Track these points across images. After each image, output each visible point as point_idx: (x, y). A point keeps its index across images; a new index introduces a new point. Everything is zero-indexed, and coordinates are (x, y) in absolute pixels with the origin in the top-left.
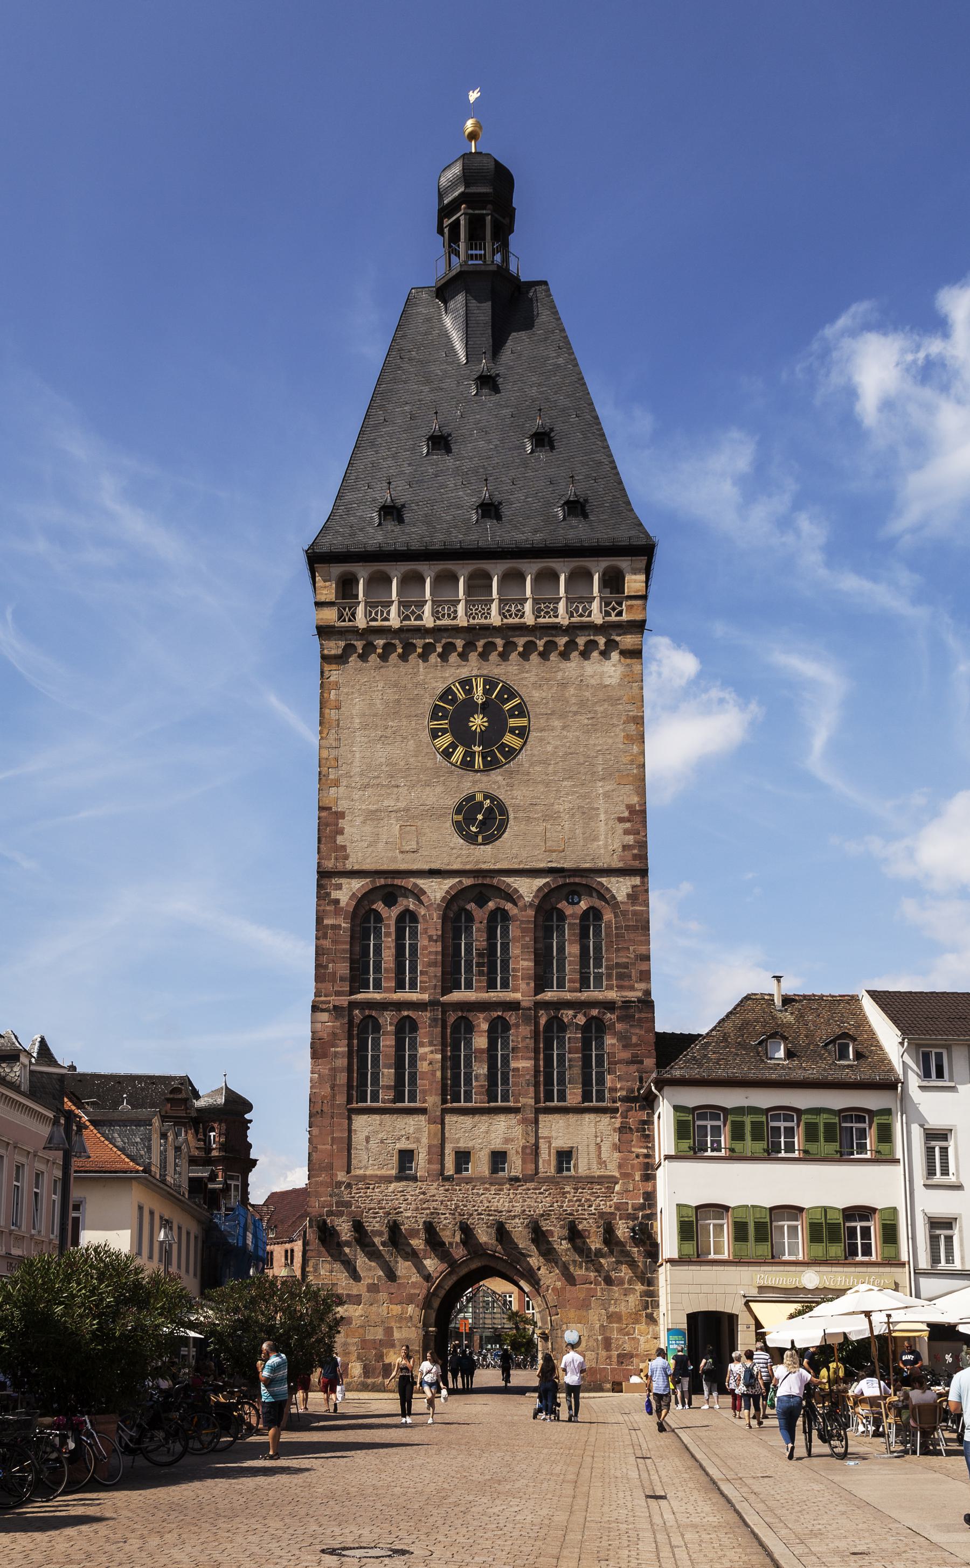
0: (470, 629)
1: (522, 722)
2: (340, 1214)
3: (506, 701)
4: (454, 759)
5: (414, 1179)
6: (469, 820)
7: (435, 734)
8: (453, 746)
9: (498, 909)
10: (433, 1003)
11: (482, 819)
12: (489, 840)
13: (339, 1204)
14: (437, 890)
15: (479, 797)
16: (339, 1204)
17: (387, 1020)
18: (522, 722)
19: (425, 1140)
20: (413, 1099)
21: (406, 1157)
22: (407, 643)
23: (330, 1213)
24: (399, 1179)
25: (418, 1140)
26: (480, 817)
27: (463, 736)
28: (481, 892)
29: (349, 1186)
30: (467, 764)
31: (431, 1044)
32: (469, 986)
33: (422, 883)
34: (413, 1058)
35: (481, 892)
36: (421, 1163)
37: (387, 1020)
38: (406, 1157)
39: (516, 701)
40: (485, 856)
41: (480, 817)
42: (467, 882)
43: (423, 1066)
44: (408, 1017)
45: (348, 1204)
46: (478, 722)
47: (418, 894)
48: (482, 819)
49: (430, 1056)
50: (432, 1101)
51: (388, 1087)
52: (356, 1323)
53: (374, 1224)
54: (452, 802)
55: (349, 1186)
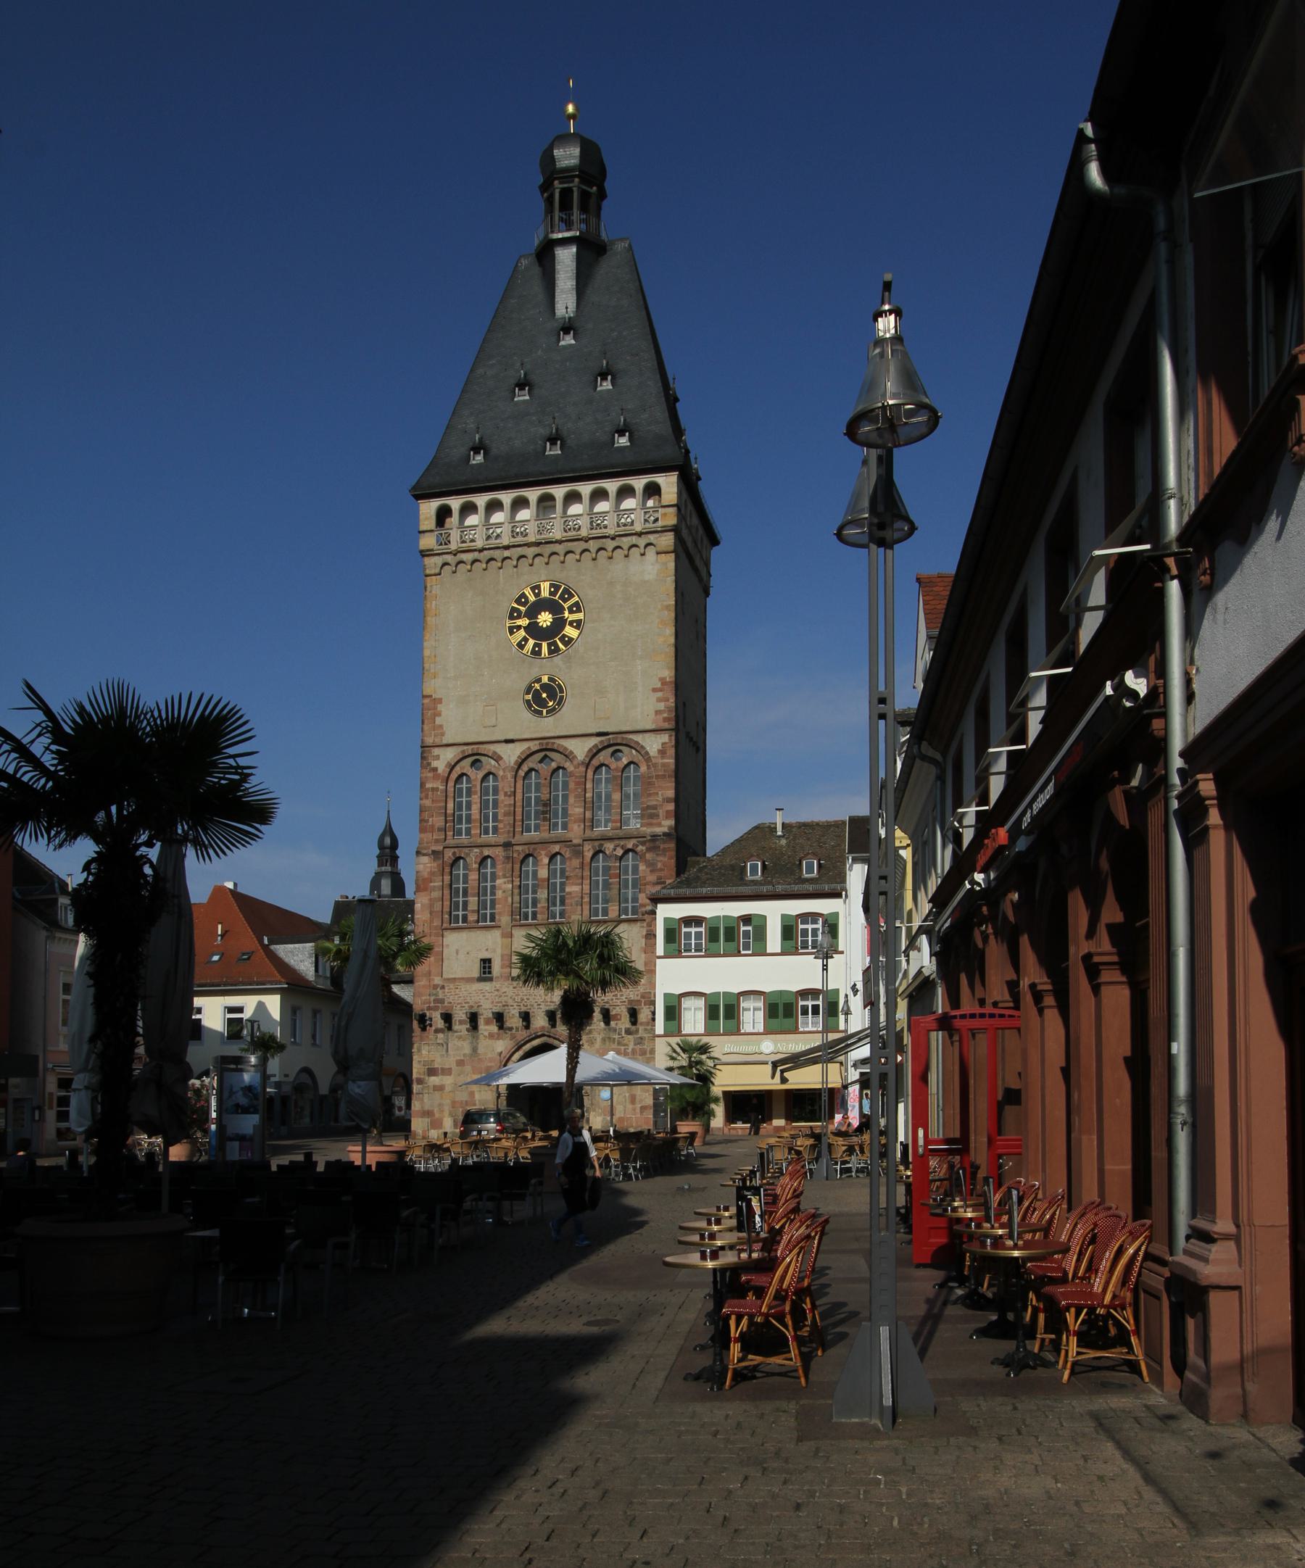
0: (538, 544)
1: (580, 616)
2: (436, 1009)
3: (565, 601)
4: (525, 651)
5: (491, 979)
6: (537, 695)
7: (511, 630)
8: (525, 640)
9: (559, 768)
10: (507, 845)
11: (545, 697)
12: (552, 711)
13: (436, 1001)
14: (511, 754)
15: (545, 679)
16: (436, 1001)
17: (473, 857)
18: (580, 616)
19: (499, 951)
20: (493, 919)
21: (486, 963)
22: (491, 556)
23: (429, 1008)
24: (481, 979)
25: (494, 951)
26: (544, 695)
27: (533, 630)
28: (546, 756)
29: (443, 987)
30: (536, 652)
31: (504, 876)
32: (537, 828)
33: (500, 749)
34: (493, 887)
35: (546, 756)
36: (496, 968)
37: (473, 857)
38: (486, 963)
39: (576, 599)
40: (547, 726)
41: (544, 695)
42: (534, 746)
43: (499, 894)
44: (488, 857)
45: (442, 1001)
46: (545, 619)
47: (498, 758)
48: (545, 697)
49: (504, 886)
50: (504, 920)
51: (473, 911)
52: (448, 1089)
53: (460, 1015)
54: (524, 686)
55: (443, 987)
